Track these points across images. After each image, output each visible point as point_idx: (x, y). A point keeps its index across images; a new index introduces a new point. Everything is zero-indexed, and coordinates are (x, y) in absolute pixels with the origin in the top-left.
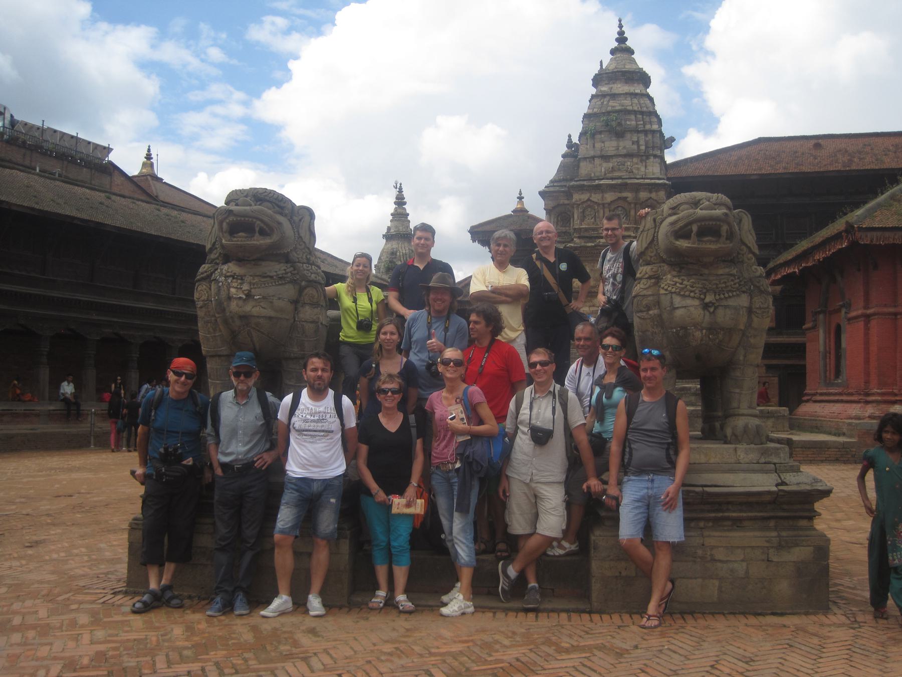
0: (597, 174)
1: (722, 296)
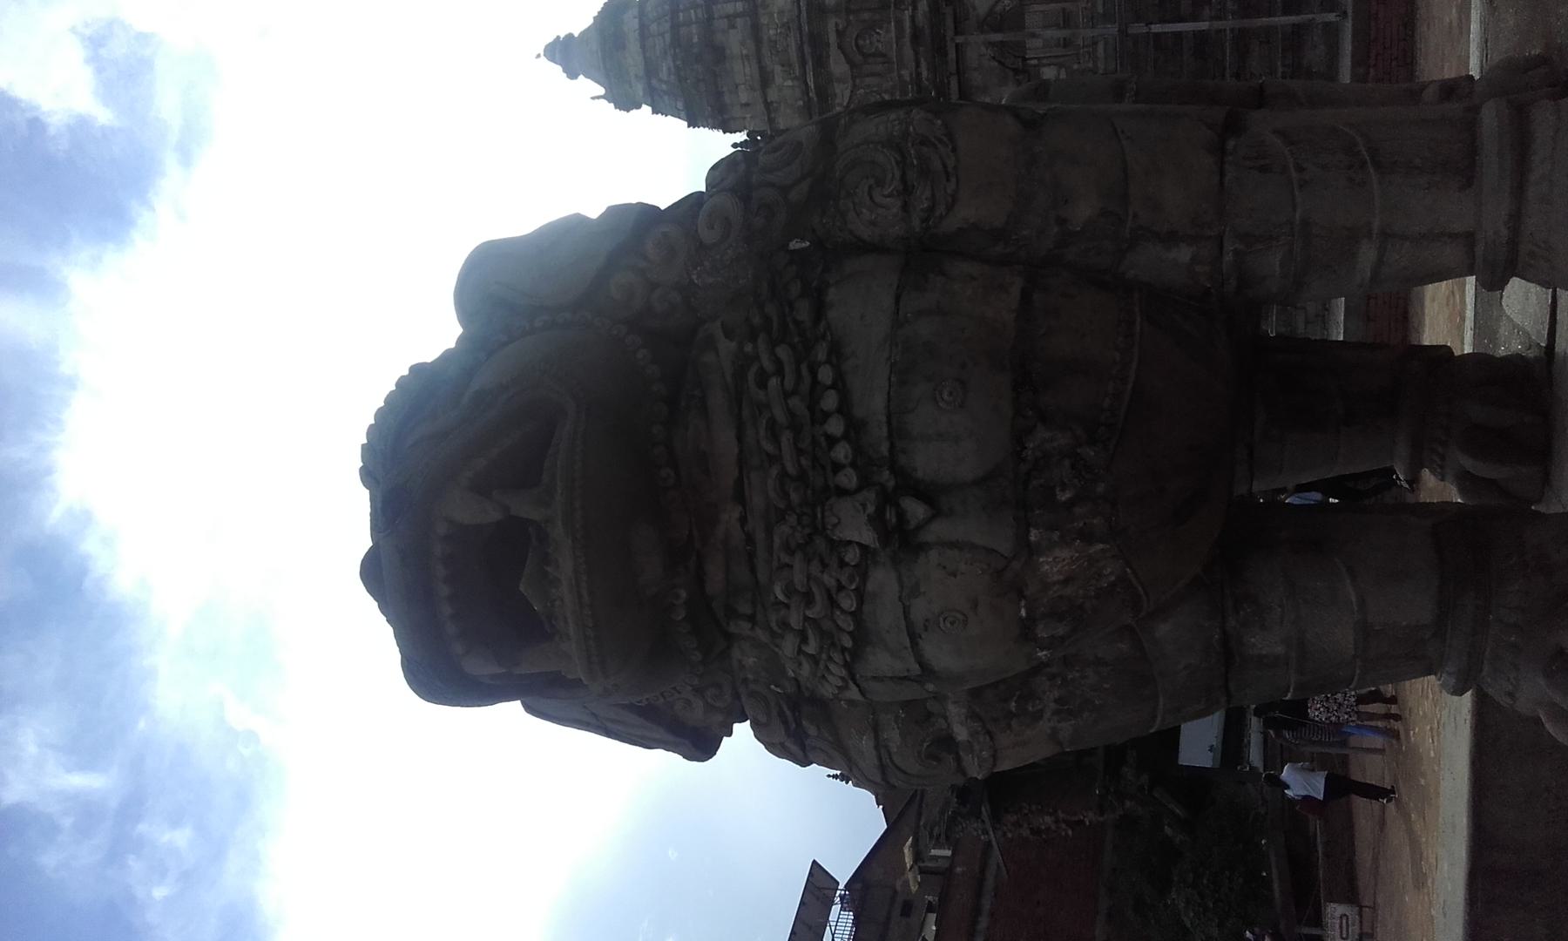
1: (842, 452)
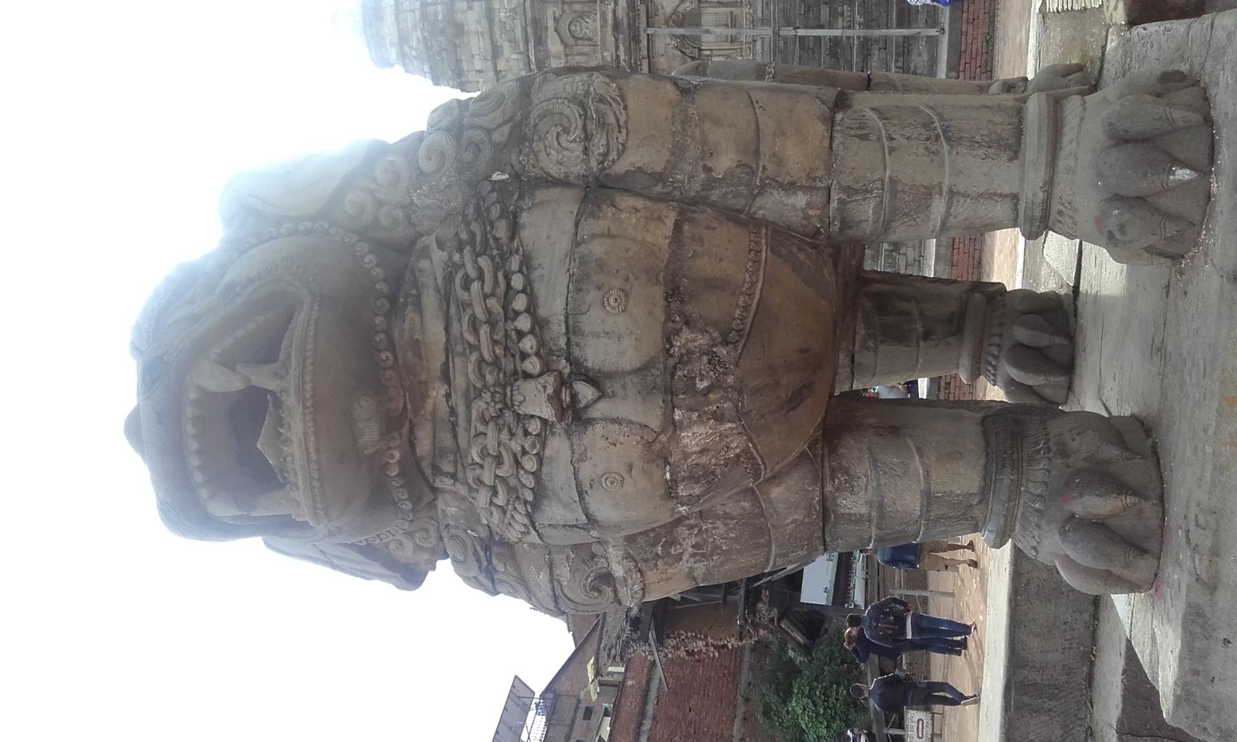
0: (521, 66)
1: (528, 344)
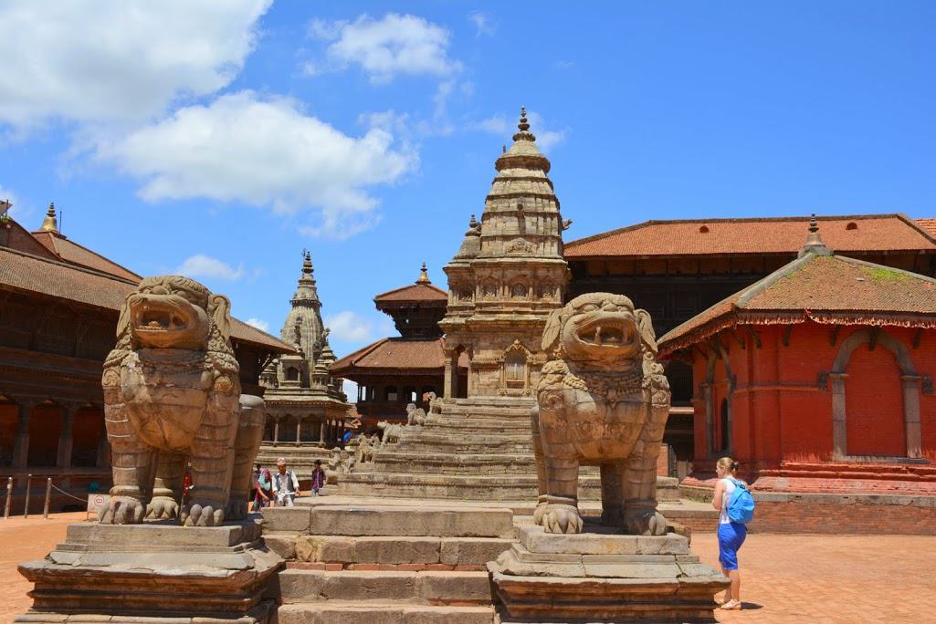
0: (499, 252)
1: (624, 393)
